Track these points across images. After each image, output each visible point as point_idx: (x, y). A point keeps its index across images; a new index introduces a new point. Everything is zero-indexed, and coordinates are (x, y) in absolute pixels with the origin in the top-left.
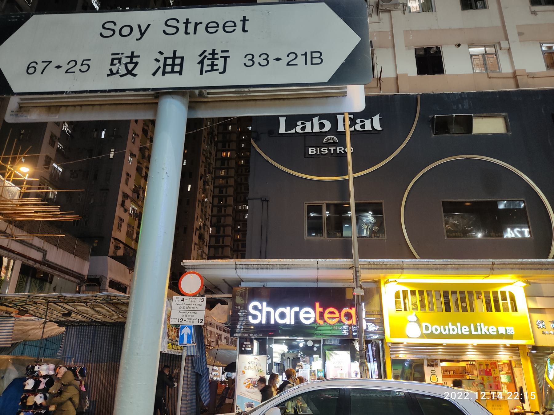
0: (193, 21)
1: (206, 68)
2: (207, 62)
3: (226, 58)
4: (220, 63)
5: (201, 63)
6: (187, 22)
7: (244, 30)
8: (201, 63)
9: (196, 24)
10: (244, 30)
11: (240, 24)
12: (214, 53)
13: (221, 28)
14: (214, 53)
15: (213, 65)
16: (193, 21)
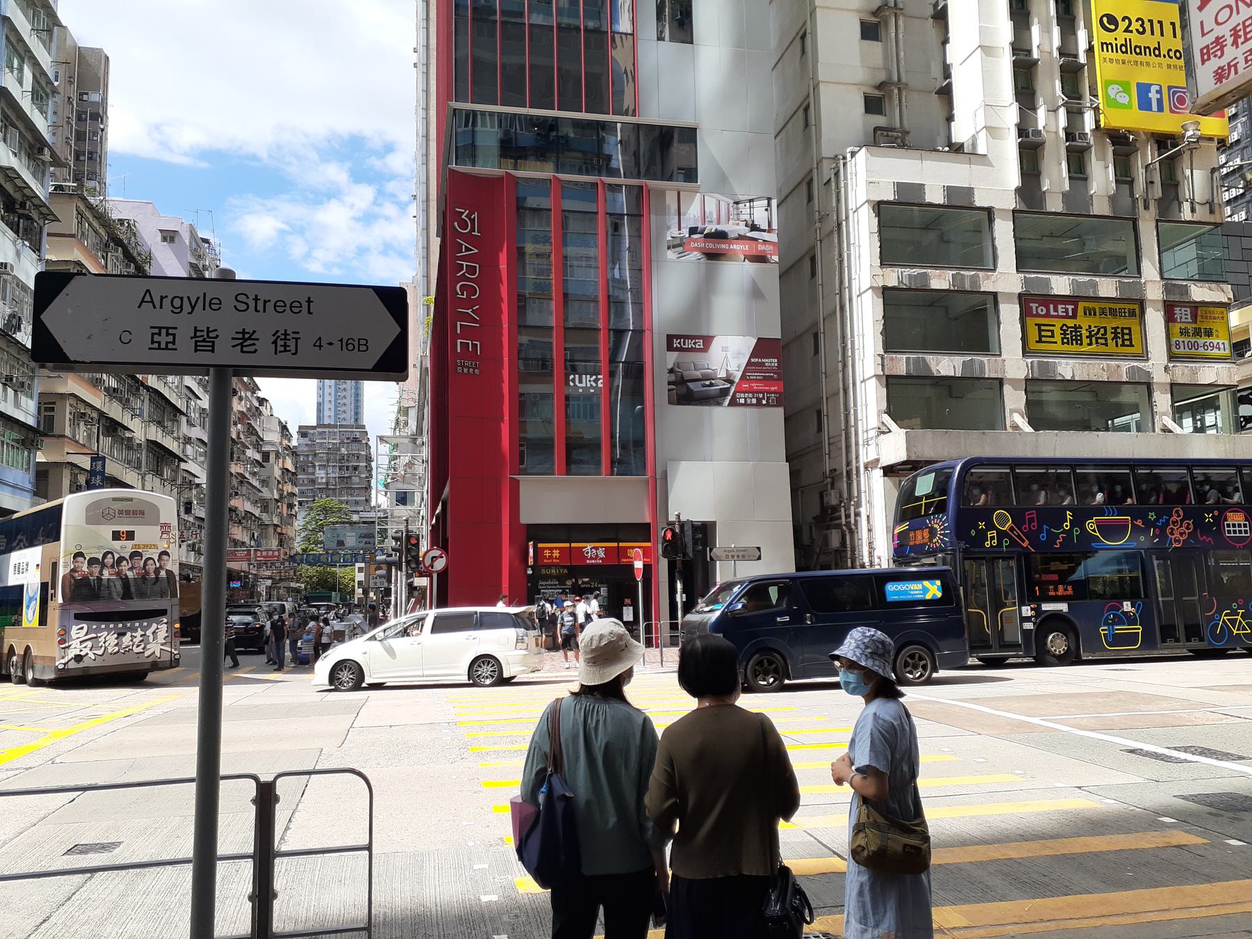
0: (262, 297)
1: (280, 348)
2: (280, 343)
3: (297, 339)
4: (292, 343)
5: (275, 342)
6: (256, 299)
7: (310, 313)
8: (275, 342)
9: (265, 302)
10: (310, 313)
11: (305, 305)
12: (286, 334)
13: (288, 308)
14: (286, 334)
15: (285, 346)
16: (262, 297)
